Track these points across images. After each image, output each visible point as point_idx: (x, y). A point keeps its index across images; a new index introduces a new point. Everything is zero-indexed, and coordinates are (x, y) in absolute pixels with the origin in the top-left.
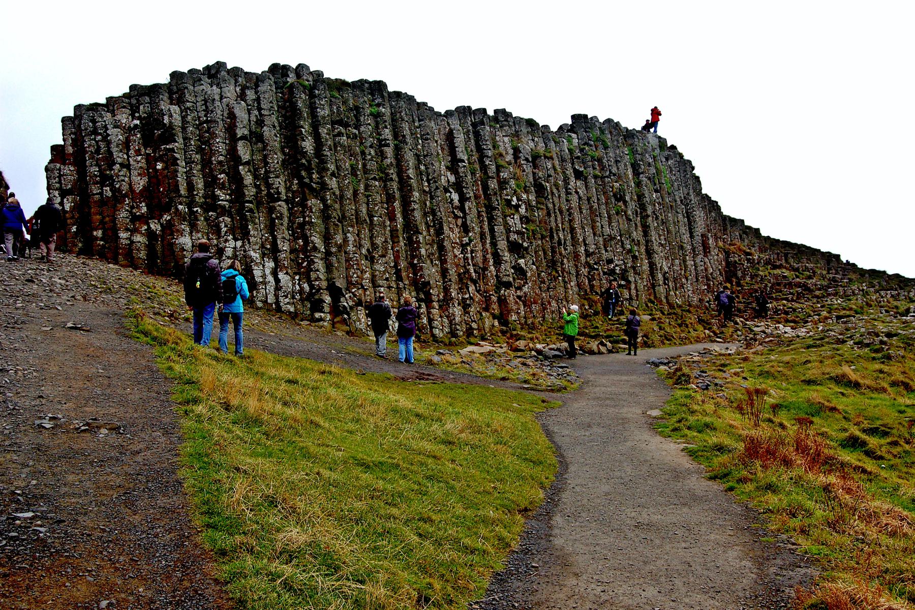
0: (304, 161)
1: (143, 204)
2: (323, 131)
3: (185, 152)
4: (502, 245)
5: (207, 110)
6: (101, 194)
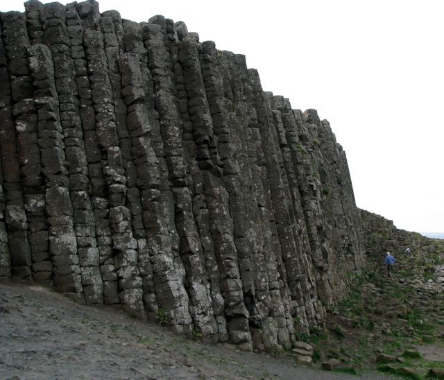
0: (207, 138)
2: (221, 102)
3: (60, 111)
4: (314, 230)
5: (86, 59)
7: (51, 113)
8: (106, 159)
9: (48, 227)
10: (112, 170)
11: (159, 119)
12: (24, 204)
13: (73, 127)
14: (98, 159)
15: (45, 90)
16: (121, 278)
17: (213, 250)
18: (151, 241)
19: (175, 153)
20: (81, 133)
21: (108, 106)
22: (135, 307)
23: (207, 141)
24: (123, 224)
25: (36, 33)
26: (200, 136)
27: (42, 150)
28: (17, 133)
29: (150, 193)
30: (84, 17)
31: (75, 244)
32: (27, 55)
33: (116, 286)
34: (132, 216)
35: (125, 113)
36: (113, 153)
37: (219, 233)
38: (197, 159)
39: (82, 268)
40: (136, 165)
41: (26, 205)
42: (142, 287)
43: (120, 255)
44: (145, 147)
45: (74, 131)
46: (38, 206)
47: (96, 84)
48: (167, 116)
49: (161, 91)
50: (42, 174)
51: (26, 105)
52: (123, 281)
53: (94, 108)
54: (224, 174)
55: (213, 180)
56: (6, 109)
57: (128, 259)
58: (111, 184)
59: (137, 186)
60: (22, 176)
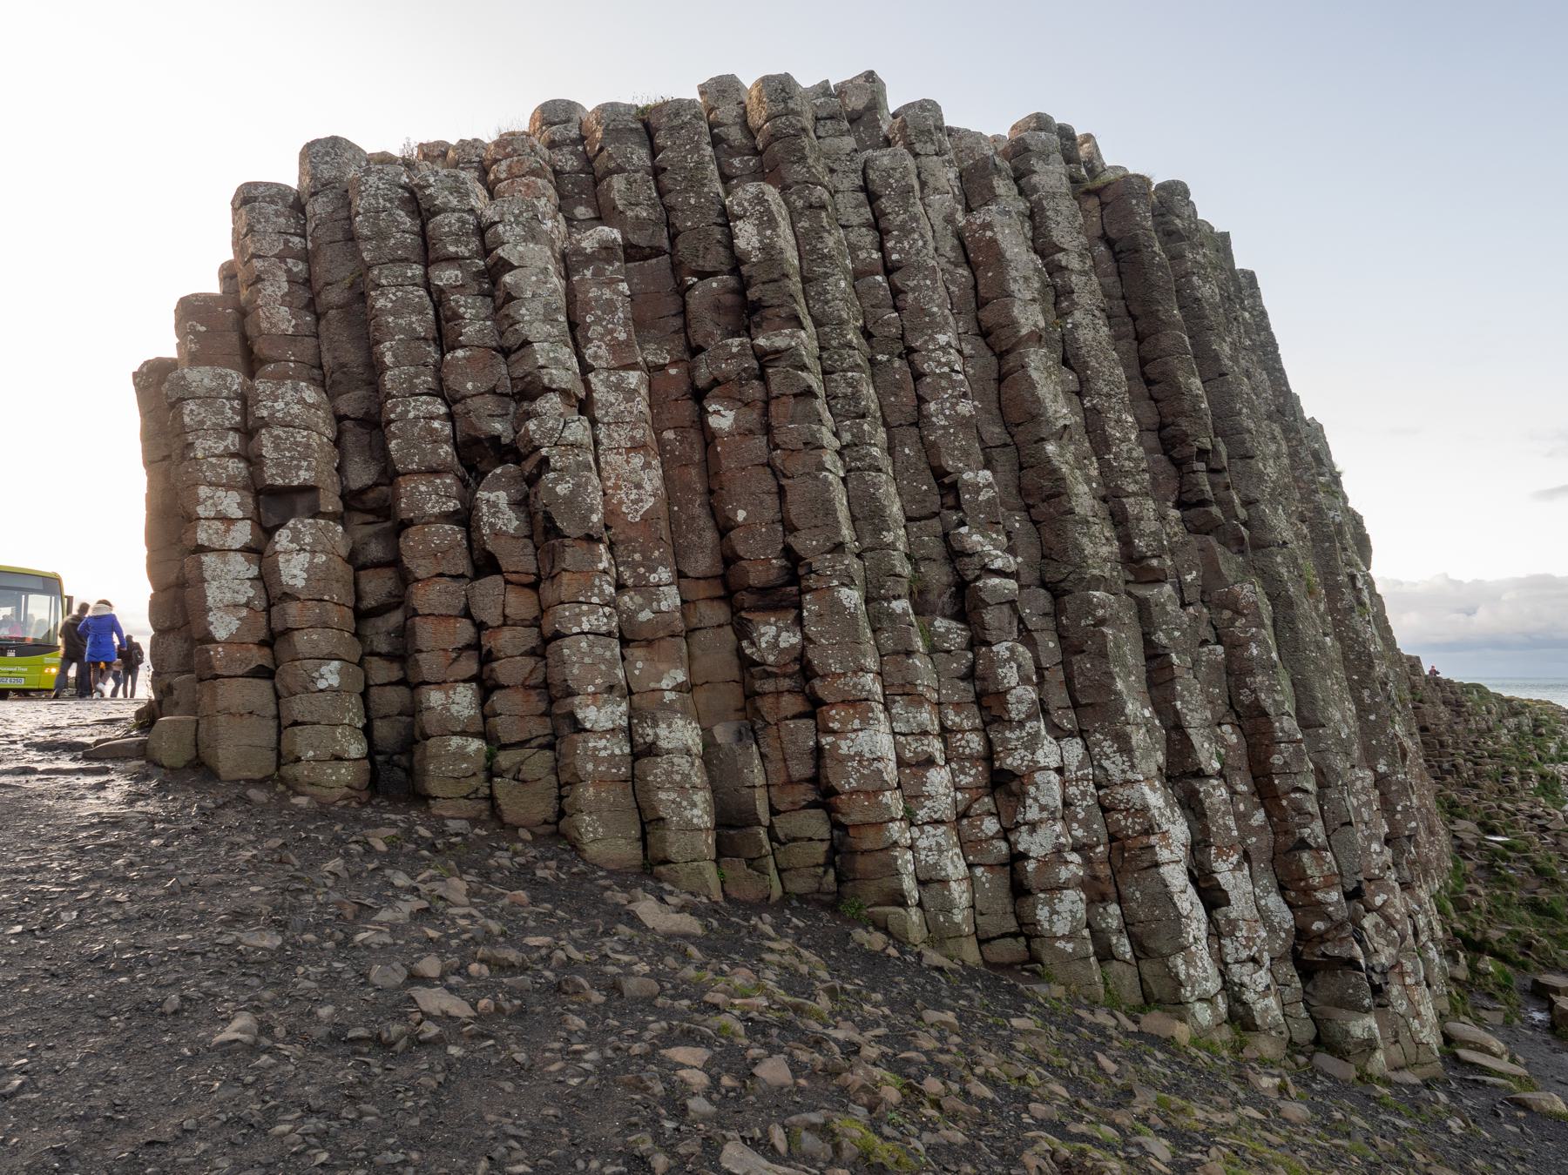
1: (664, 574)
3: (825, 372)
5: (878, 226)
6: (465, 517)
7: (804, 375)
8: (958, 507)
9: (814, 707)
10: (976, 538)
11: (1078, 394)
12: (739, 640)
13: (863, 416)
14: (935, 509)
15: (783, 313)
16: (1024, 856)
17: (1244, 765)
18: (1098, 744)
19: (1132, 488)
20: (882, 434)
21: (947, 347)
22: (1069, 947)
23: (1207, 451)
24: (1022, 697)
25: (736, 162)
26: (1183, 439)
27: (784, 482)
28: (709, 438)
29: (1091, 602)
30: (855, 118)
31: (893, 757)
32: (727, 218)
33: (1008, 882)
34: (1039, 670)
35: (995, 375)
36: (977, 489)
37: (1266, 714)
38: (1179, 505)
39: (914, 829)
40: (1035, 523)
41: (745, 644)
42: (1082, 885)
43: (1014, 786)
44: (1065, 469)
45: (866, 427)
46: (783, 645)
47: (910, 297)
48: (1101, 384)
49: (1078, 315)
50: (788, 552)
51: (733, 356)
52: (1031, 866)
53: (911, 364)
54: (1254, 544)
55: (1229, 563)
56: (673, 371)
57: (1043, 801)
58: (978, 578)
59: (1043, 584)
60: (730, 559)
